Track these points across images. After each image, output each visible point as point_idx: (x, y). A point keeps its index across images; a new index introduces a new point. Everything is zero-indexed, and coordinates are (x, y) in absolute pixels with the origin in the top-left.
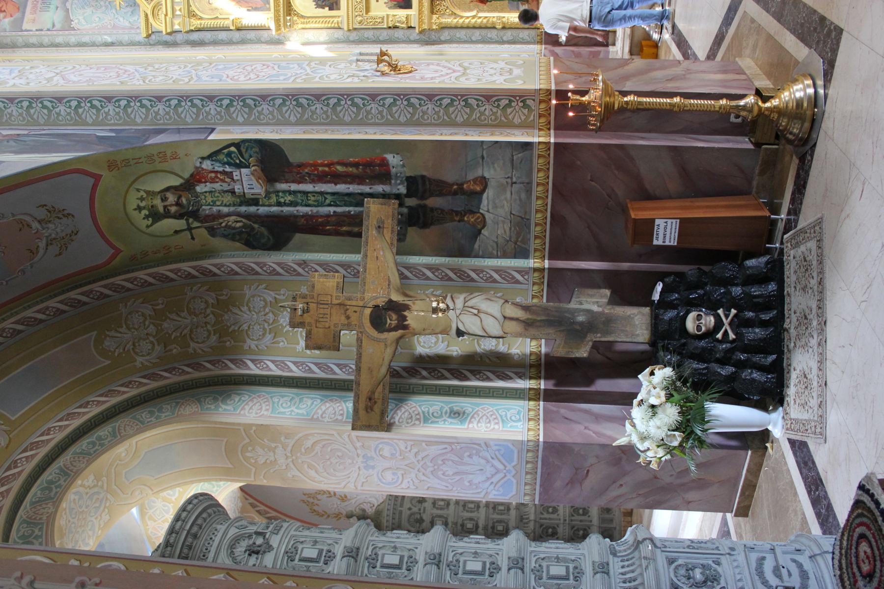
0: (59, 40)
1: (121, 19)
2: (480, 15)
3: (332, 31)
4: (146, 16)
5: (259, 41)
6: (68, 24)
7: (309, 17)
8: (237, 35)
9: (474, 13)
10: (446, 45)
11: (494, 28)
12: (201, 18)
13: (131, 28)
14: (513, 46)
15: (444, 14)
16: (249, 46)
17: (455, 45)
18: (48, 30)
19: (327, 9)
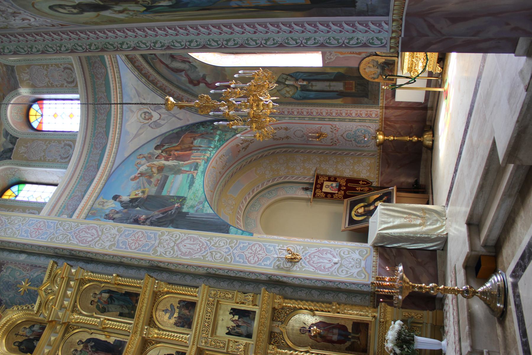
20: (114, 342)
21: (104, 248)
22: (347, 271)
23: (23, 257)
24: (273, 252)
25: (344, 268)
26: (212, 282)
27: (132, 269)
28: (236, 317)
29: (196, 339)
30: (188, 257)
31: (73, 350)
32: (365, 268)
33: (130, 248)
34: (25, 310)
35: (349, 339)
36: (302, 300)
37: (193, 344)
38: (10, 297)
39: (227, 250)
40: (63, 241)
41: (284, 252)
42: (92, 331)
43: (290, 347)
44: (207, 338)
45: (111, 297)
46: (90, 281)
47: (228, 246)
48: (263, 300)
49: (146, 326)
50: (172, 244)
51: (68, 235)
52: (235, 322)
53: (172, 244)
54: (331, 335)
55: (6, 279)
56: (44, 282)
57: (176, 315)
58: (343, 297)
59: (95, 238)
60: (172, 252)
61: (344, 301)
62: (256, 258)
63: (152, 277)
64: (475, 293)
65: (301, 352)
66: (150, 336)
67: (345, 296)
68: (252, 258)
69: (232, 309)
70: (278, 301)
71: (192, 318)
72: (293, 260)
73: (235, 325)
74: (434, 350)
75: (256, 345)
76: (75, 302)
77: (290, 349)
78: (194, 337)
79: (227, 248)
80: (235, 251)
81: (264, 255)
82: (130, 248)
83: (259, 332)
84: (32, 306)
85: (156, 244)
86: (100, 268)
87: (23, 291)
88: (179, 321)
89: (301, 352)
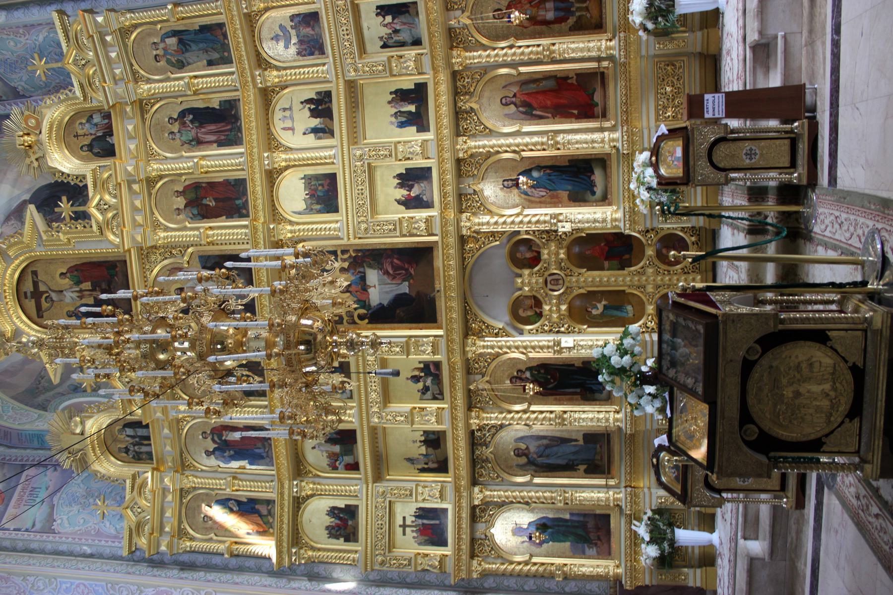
0: (34, 546)
1: (108, 524)
3: (350, 567)
4: (131, 530)
5: (258, 570)
6: (48, 528)
7: (319, 550)
8: (234, 561)
12: (192, 539)
13: (115, 537)
18: (27, 530)
19: (342, 539)
20: (220, 105)
28: (389, 19)
29: (338, 61)
31: (167, 135)
34: (65, 100)
35: (573, 13)
37: (337, 79)
38: (24, 79)
42: (180, 99)
43: (484, 45)
44: (355, 63)
45: (181, 42)
46: (135, 26)
49: (256, 69)
52: (389, 26)
54: (543, 13)
56: (65, 51)
57: (294, 40)
65: (503, 48)
66: (269, 84)
69: (378, 7)
71: (321, 37)
73: (390, 31)
74: (707, 12)
75: (433, 57)
76: (132, 65)
77: (485, 48)
78: (336, 68)
84: (70, 91)
87: (42, 74)
88: (304, 47)
89: (503, 48)
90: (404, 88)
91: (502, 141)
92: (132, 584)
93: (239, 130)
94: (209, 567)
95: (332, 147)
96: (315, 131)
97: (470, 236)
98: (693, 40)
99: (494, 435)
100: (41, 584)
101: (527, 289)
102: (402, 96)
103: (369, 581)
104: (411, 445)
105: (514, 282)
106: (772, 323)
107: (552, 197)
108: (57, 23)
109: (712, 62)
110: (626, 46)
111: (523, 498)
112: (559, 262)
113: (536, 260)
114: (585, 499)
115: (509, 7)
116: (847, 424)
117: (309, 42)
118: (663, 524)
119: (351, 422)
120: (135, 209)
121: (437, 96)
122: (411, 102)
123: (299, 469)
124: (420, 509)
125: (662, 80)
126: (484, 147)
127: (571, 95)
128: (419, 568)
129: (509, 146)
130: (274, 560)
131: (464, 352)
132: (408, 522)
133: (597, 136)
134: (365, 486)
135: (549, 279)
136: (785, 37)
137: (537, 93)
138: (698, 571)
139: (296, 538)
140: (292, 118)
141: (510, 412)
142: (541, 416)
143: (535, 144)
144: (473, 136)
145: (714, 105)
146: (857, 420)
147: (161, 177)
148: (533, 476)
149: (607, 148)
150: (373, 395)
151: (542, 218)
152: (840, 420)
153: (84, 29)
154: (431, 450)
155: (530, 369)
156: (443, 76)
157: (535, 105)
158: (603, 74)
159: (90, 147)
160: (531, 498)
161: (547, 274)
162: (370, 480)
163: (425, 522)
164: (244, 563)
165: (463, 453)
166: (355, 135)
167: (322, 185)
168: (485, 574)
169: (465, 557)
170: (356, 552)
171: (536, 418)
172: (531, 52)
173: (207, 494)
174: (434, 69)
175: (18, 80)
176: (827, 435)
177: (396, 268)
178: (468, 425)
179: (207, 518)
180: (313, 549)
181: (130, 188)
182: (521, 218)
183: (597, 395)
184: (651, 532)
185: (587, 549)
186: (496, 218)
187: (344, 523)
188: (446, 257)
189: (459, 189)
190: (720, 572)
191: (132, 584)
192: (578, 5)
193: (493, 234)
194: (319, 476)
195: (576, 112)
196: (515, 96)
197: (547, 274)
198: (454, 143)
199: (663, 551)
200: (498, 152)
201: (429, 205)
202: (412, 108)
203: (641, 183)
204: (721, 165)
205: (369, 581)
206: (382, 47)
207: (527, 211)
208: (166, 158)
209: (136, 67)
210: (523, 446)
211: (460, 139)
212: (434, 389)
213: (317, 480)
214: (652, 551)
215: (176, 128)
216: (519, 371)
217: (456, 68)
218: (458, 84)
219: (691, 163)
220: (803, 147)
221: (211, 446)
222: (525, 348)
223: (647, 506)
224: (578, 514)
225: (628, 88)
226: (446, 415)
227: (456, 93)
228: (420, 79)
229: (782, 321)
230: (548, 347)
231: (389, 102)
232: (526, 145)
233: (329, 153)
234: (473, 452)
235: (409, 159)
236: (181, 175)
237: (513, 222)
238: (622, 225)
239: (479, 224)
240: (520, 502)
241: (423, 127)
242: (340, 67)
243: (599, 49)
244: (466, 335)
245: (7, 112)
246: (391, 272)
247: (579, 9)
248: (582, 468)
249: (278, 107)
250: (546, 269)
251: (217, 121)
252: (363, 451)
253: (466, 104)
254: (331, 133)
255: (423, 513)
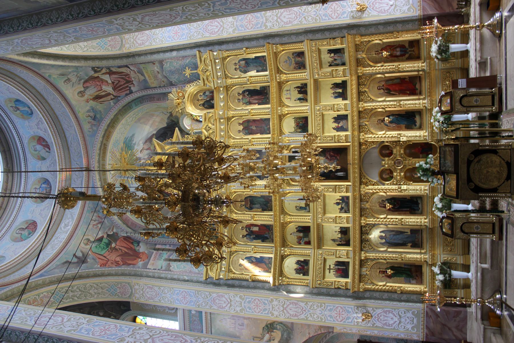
0: (163, 275)
2: (388, 284)
5: (263, 288)
6: (168, 269)
7: (291, 279)
8: (252, 284)
9: (384, 283)
10: (368, 301)
11: (396, 292)
14: (407, 304)
15: (367, 283)
16: (257, 291)
17: (373, 301)
18: (159, 270)
19: (302, 275)
21: (230, 34)
22: (400, 10)
23: (174, 54)
24: (347, 7)
25: (398, 8)
26: (310, 36)
27: (253, 41)
28: (332, 55)
30: (290, 25)
32: (413, 4)
33: (248, 29)
35: (408, 53)
36: (373, 34)
37: (311, 78)
39: (315, 13)
40: (199, 37)
41: (356, 5)
45: (246, 63)
46: (228, 56)
47: (314, 10)
48: (348, 41)
50: (275, 18)
51: (200, 32)
53: (275, 18)
55: (169, 69)
57: (293, 62)
58: (399, 27)
59: (220, 28)
60: (277, 24)
61: (401, 29)
62: (336, 14)
63: (269, 43)
64: (483, 26)
66: (282, 80)
67: (401, 25)
68: (333, 14)
69: (328, 50)
70: (358, 39)
72: (362, 10)
75: (350, 70)
76: (225, 72)
77: (371, 66)
79: (314, 11)
80: (320, 12)
81: (341, 10)
82: (248, 29)
83: (350, 61)
85: (264, 21)
86: (231, 46)
90: (338, 82)
91: (378, 104)
92: (207, 292)
93: (268, 98)
94: (240, 287)
95: (307, 106)
96: (300, 99)
97: (363, 143)
98: (458, 63)
99: (371, 229)
100: (166, 291)
101: (387, 166)
102: (336, 85)
103: (313, 293)
104: (335, 233)
105: (381, 163)
106: (477, 146)
107: (398, 127)
108: (198, 56)
109: (466, 71)
110: (430, 65)
111: (383, 257)
112: (400, 155)
113: (391, 154)
114: (411, 258)
115: (382, 50)
116: (506, 183)
117: (299, 64)
118: (446, 267)
119: (309, 222)
120: (221, 130)
121: (352, 85)
122: (340, 88)
123: (284, 243)
124: (337, 262)
125: (444, 79)
126: (370, 106)
127: (407, 86)
128: (336, 287)
129: (380, 106)
130: (271, 282)
131: (360, 191)
132: (332, 267)
133: (417, 102)
134: (313, 250)
135: (396, 162)
136: (491, 59)
137: (393, 85)
138: (462, 291)
139: (281, 273)
140: (290, 94)
141: (378, 218)
142: (392, 220)
143: (391, 105)
144: (366, 102)
145: (462, 83)
146: (509, 181)
147: (233, 117)
148: (388, 248)
149: (421, 107)
150: (320, 210)
151: (394, 135)
152: (503, 181)
153: (209, 58)
154: (343, 236)
155: (387, 200)
156: (354, 78)
157: (392, 90)
158: (420, 77)
159: (203, 105)
160: (387, 257)
161: (395, 160)
162: (316, 247)
163: (339, 267)
164: (256, 284)
165: (358, 236)
166: (317, 101)
167: (302, 121)
168: (366, 290)
169: (357, 281)
170: (308, 280)
171: (390, 221)
172: (390, 68)
173: (242, 254)
174: (351, 74)
175: (174, 78)
176: (499, 187)
177: (331, 156)
178: (360, 223)
179: (241, 265)
180: (288, 278)
181: (220, 121)
182: (385, 135)
183: (417, 212)
184: (440, 270)
185: (411, 280)
186: (374, 136)
187: (303, 267)
188: (354, 151)
189: (359, 122)
190: (472, 289)
191: (207, 292)
192: (409, 49)
193: (373, 142)
194: (292, 247)
195: (408, 92)
196: (383, 86)
197: (395, 160)
198: (358, 104)
199: (445, 279)
200: (376, 108)
201: (346, 130)
202: (340, 91)
203: (435, 120)
204: (465, 105)
205: (313, 293)
206: (329, 66)
207: (387, 133)
208: (236, 109)
209: (227, 72)
210: (384, 235)
211: (361, 103)
212: (345, 208)
213: (292, 248)
214: (441, 277)
215: (241, 97)
216: (383, 201)
217: (359, 74)
218: (360, 81)
219: (453, 104)
220: (497, 98)
221: (245, 233)
222: (386, 190)
223: (439, 260)
224: (408, 265)
225: (430, 82)
226: (351, 220)
227: (359, 84)
228: (344, 79)
229: (481, 146)
230: (396, 190)
231: (331, 88)
232: (388, 105)
233: (304, 109)
234: (361, 237)
235: (339, 111)
236: (242, 116)
237: (382, 137)
238: (427, 138)
239: (368, 138)
240: (382, 259)
241: (345, 98)
242: (312, 74)
243: (418, 67)
244: (361, 184)
245: (169, 91)
246: (329, 158)
247: (410, 51)
248: (410, 245)
249: (284, 89)
250: (395, 157)
251: (260, 95)
252: (313, 235)
253: (363, 89)
254: (306, 100)
255: (338, 263)
